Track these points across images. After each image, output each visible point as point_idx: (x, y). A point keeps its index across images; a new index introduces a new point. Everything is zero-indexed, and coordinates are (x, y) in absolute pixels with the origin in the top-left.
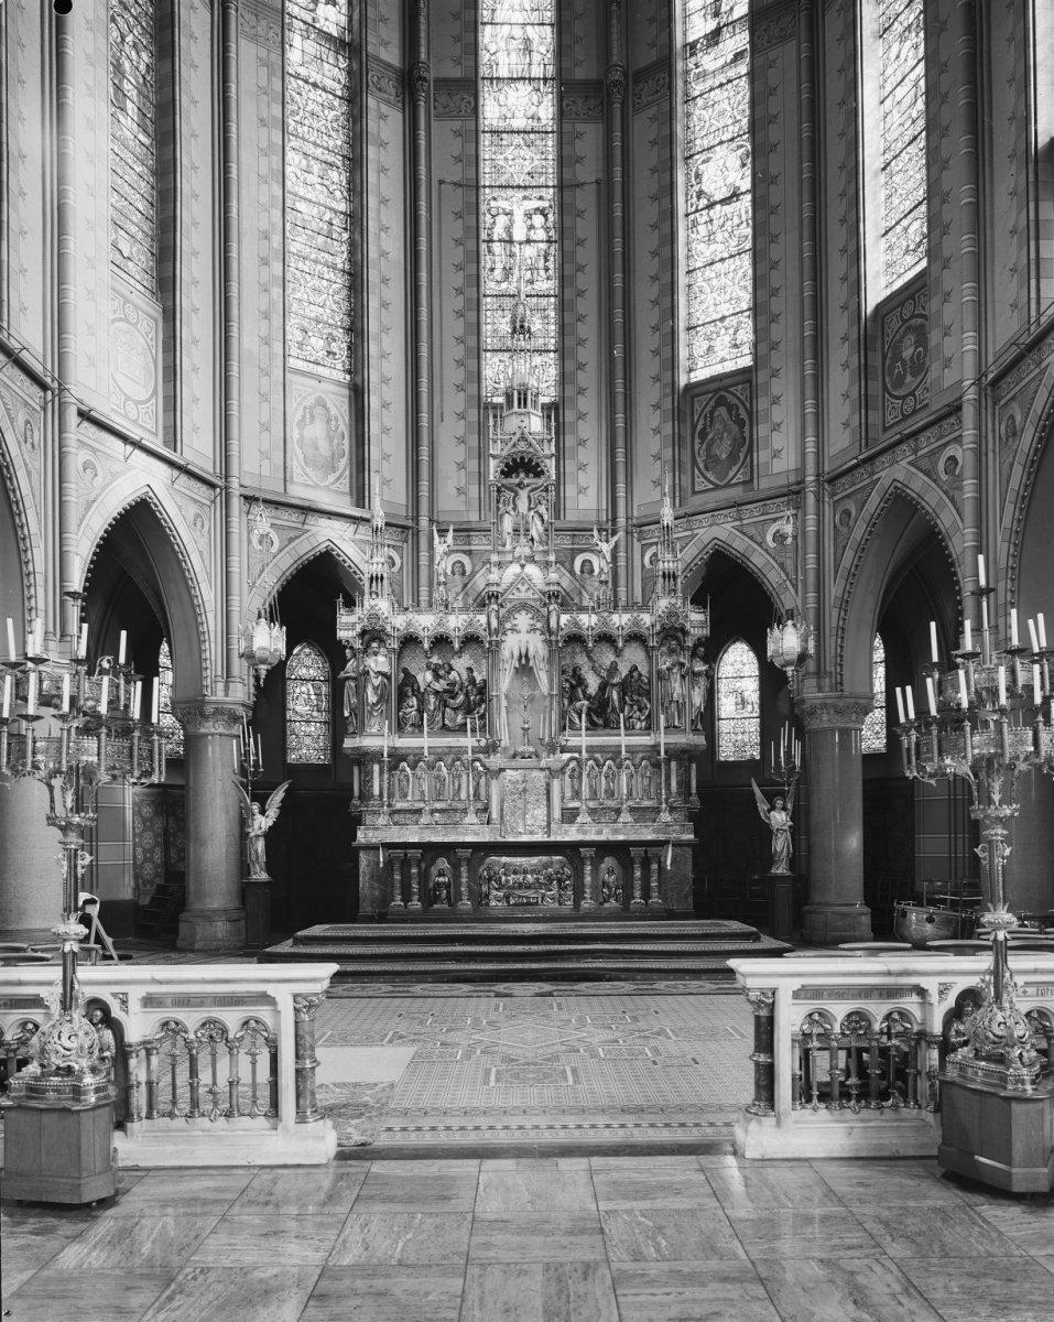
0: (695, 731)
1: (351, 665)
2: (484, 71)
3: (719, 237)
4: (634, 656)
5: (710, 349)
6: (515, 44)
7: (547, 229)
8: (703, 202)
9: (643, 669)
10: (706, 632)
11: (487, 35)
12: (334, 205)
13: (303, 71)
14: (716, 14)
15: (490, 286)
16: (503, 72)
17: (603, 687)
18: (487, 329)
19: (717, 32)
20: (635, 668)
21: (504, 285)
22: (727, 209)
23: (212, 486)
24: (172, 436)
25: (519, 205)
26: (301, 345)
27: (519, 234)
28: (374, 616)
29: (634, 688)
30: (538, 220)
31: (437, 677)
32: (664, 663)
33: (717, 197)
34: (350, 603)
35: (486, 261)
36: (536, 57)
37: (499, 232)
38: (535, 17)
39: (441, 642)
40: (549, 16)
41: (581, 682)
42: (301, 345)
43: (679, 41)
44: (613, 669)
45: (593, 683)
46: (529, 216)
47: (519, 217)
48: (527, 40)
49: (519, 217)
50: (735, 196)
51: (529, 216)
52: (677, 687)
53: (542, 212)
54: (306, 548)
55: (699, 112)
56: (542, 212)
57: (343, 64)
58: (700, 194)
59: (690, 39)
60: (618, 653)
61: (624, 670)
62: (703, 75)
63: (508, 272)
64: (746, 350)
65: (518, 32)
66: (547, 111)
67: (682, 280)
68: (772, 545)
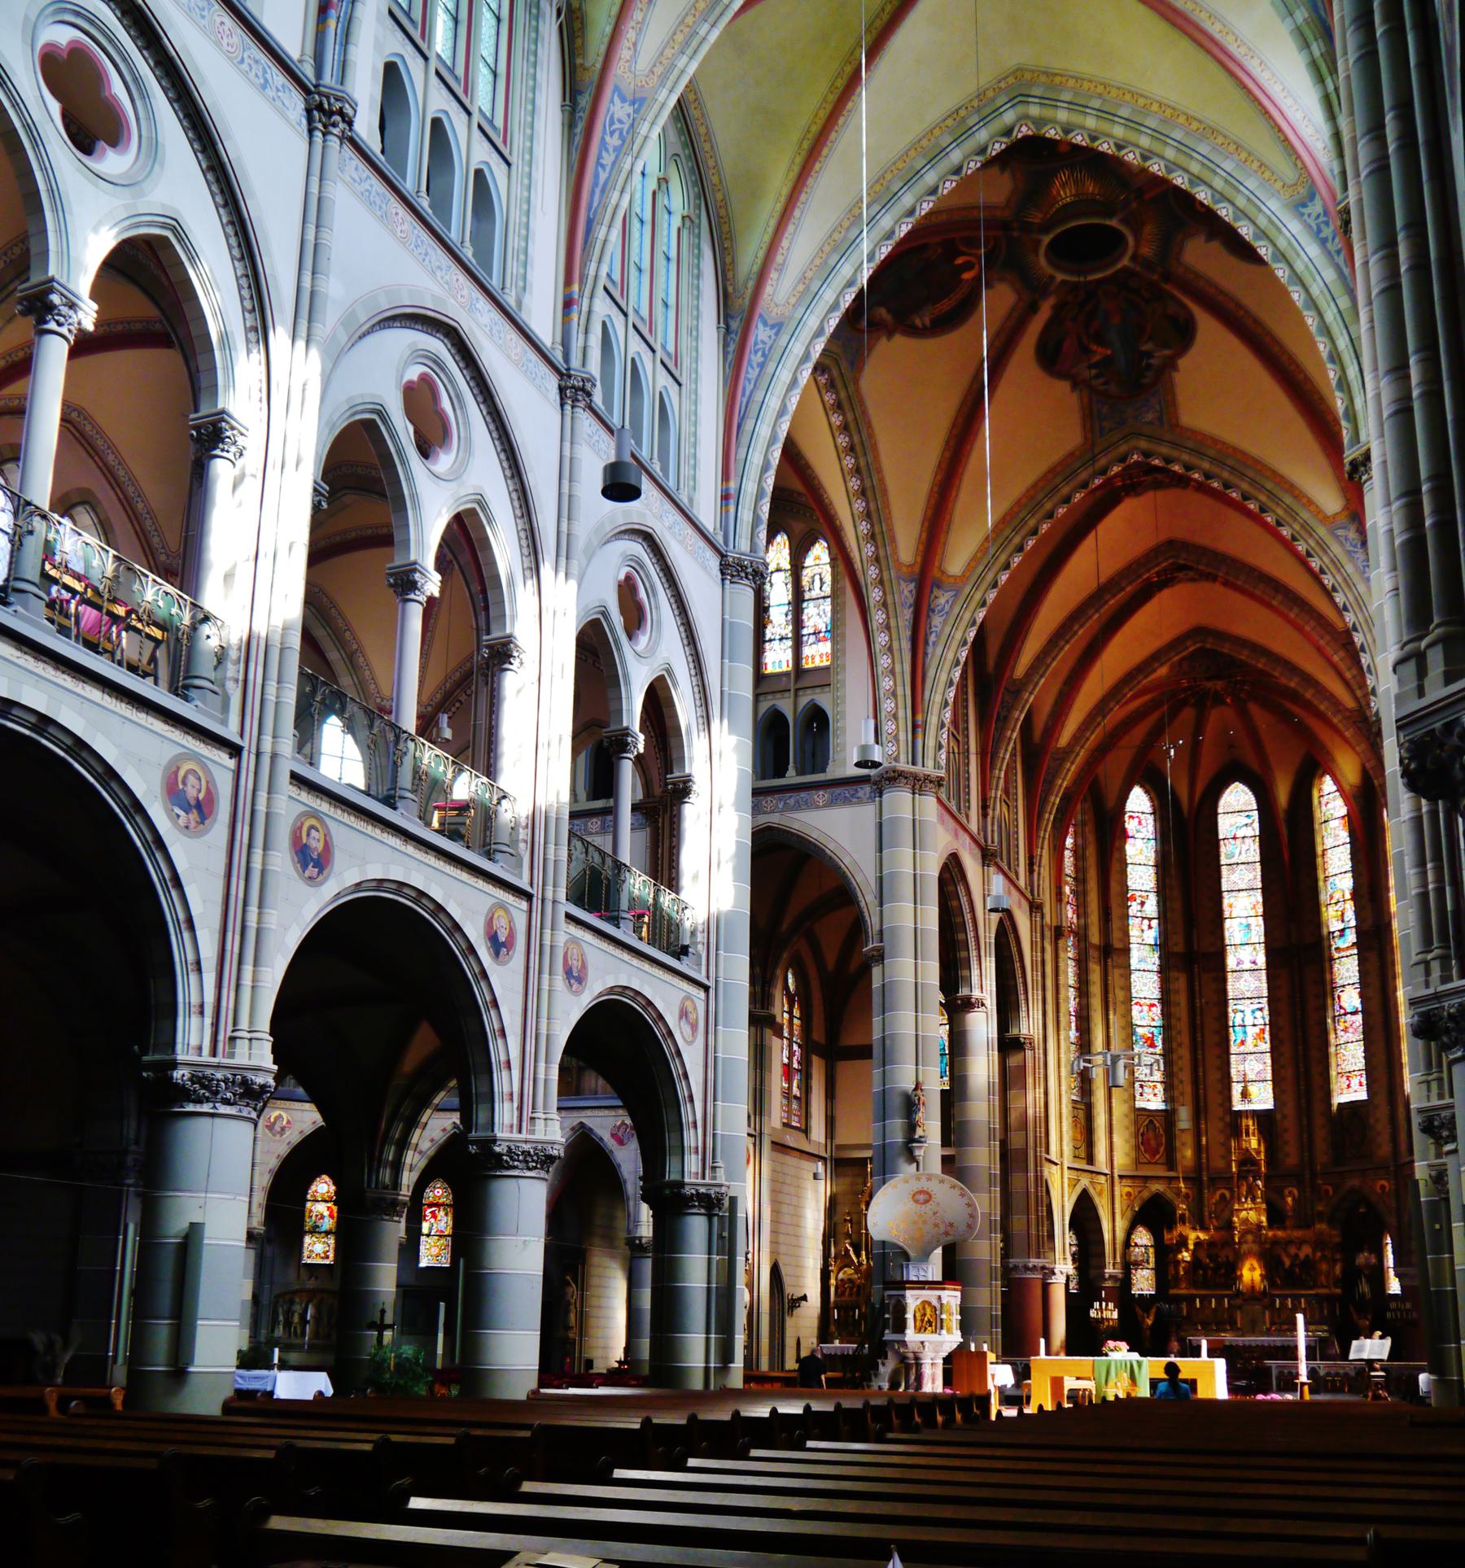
0: (1336, 1287)
1: (1171, 1255)
2: (1227, 942)
3: (1351, 1030)
4: (1306, 1251)
5: (1349, 1086)
6: (1242, 928)
7: (1263, 1018)
8: (1342, 1011)
9: (1311, 1256)
10: (1337, 1240)
11: (1228, 923)
12: (1154, 1024)
13: (1138, 967)
14: (1343, 921)
15: (1234, 1049)
16: (1238, 942)
17: (1292, 1265)
18: (1233, 1072)
19: (1342, 931)
20: (1307, 1256)
21: (1242, 1048)
22: (1354, 1018)
23: (1106, 1175)
24: (1090, 1159)
25: (1247, 1007)
26: (1141, 1095)
27: (1249, 1021)
28: (1181, 1235)
29: (1308, 1264)
30: (1258, 1014)
31: (1211, 1261)
32: (1319, 1254)
33: (1349, 1010)
34: (1170, 1229)
35: (1232, 1037)
36: (1254, 933)
37: (1238, 1021)
38: (1253, 913)
39: (1211, 1244)
40: (1260, 910)
41: (1282, 1263)
42: (1141, 1095)
43: (1325, 931)
44: (1297, 1255)
45: (1287, 1262)
46: (1253, 1012)
47: (1248, 1013)
48: (1249, 925)
49: (1248, 1013)
50: (1354, 1013)
51: (1253, 1012)
52: (1324, 1267)
53: (1261, 1009)
54: (1146, 1195)
55: (1336, 966)
56: (1261, 1009)
57: (1157, 955)
58: (1341, 1007)
59: (1332, 930)
60: (1299, 1249)
61: (1302, 1255)
62: (1338, 949)
63: (1243, 1043)
64: (1365, 1088)
65: (1244, 921)
66: (1261, 960)
67: (1332, 1050)
68: (1379, 1191)
